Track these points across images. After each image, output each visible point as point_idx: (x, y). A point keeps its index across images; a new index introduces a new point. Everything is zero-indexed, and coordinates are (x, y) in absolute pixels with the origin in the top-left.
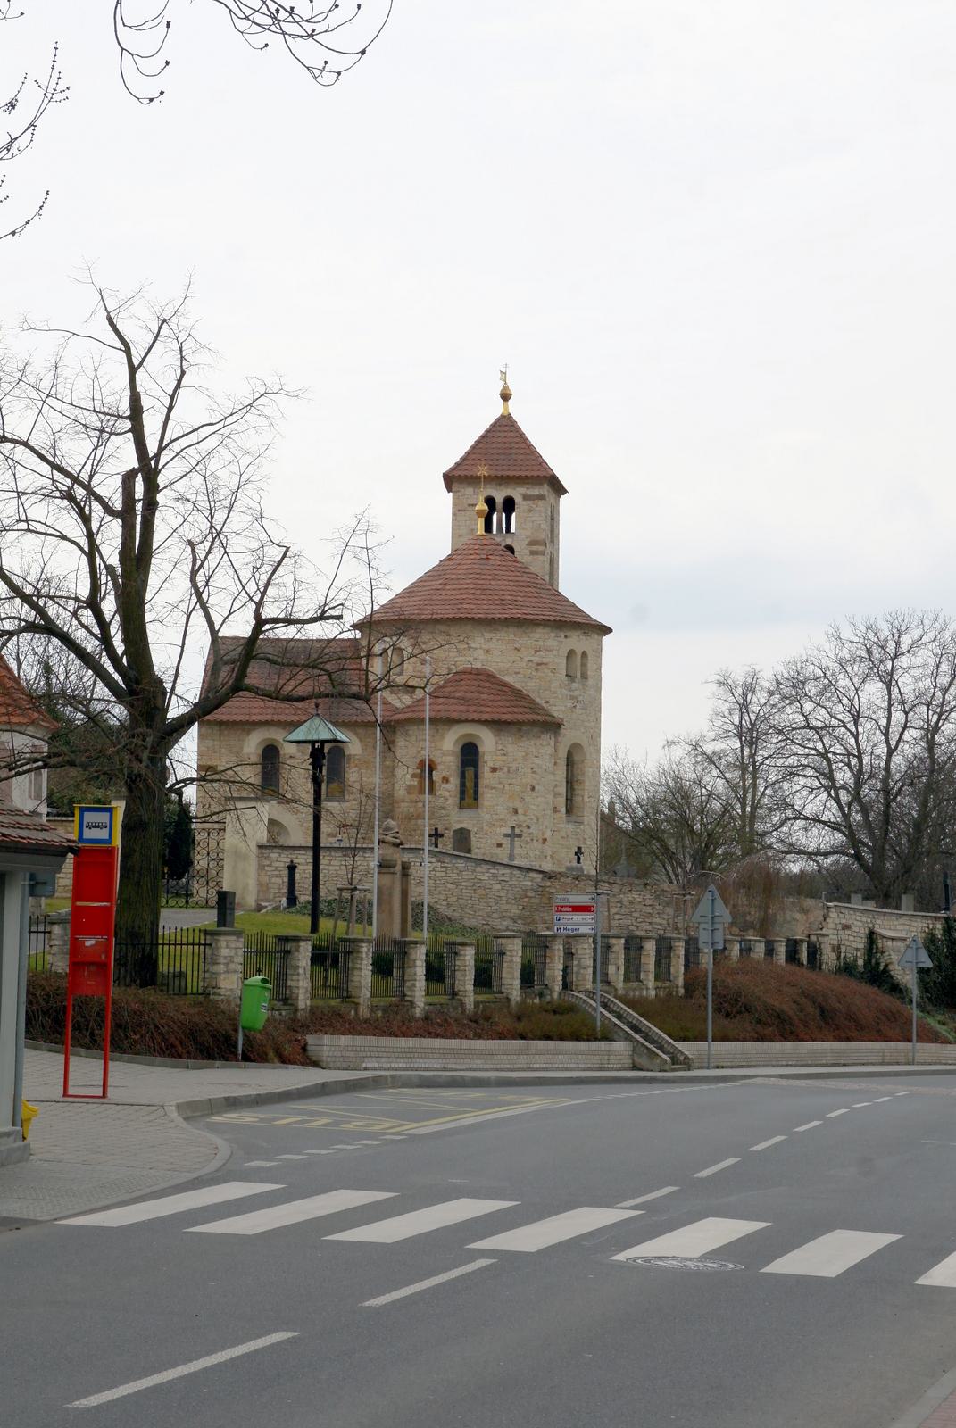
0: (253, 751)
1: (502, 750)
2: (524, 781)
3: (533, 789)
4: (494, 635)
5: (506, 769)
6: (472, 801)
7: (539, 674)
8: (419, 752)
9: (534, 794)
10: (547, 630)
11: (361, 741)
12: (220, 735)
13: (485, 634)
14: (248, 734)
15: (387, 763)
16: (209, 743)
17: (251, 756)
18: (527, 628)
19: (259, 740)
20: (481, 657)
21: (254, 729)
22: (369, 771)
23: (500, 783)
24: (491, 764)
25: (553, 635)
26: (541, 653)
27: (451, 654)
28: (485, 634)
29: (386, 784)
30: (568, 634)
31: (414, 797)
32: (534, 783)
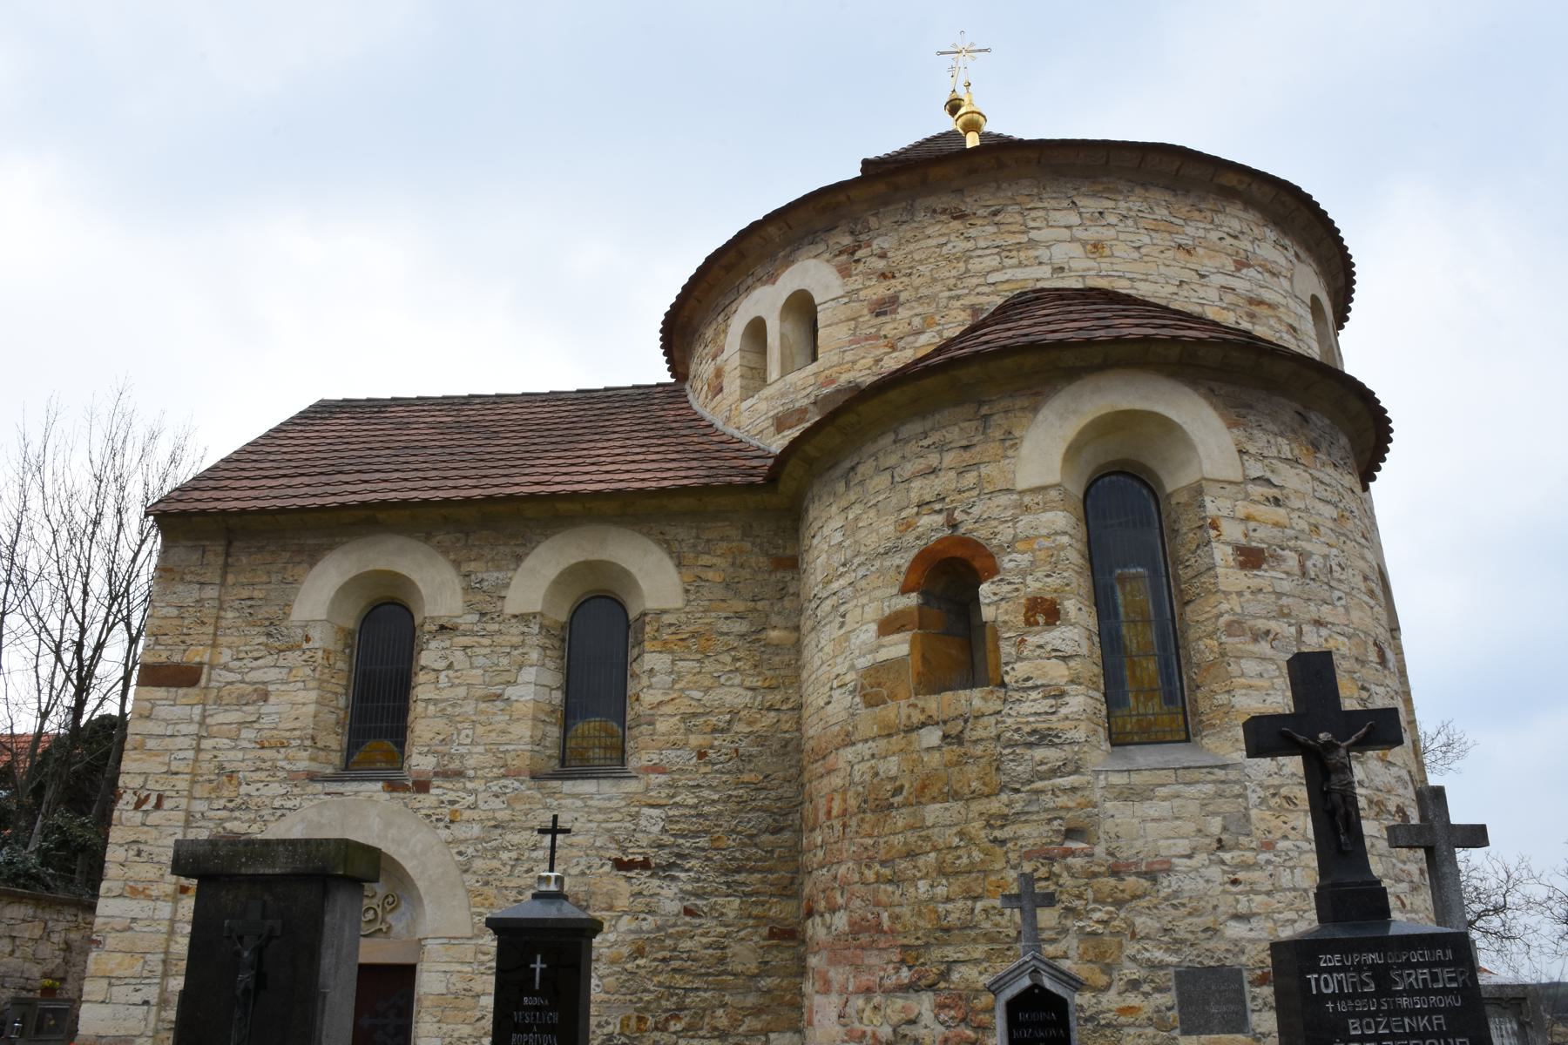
0: (321, 613)
2: (1356, 615)
4: (1111, 204)
6: (1154, 706)
8: (907, 525)
10: (1251, 216)
11: (679, 565)
12: (226, 566)
13: (1081, 201)
14: (312, 566)
15: (774, 634)
16: (187, 594)
17: (316, 634)
18: (1203, 199)
19: (347, 578)
20: (1075, 264)
21: (331, 548)
22: (709, 666)
23: (1283, 614)
24: (1233, 532)
26: (1251, 272)
27: (975, 265)
28: (1081, 201)
29: (770, 709)
30: (1303, 254)
31: (898, 710)
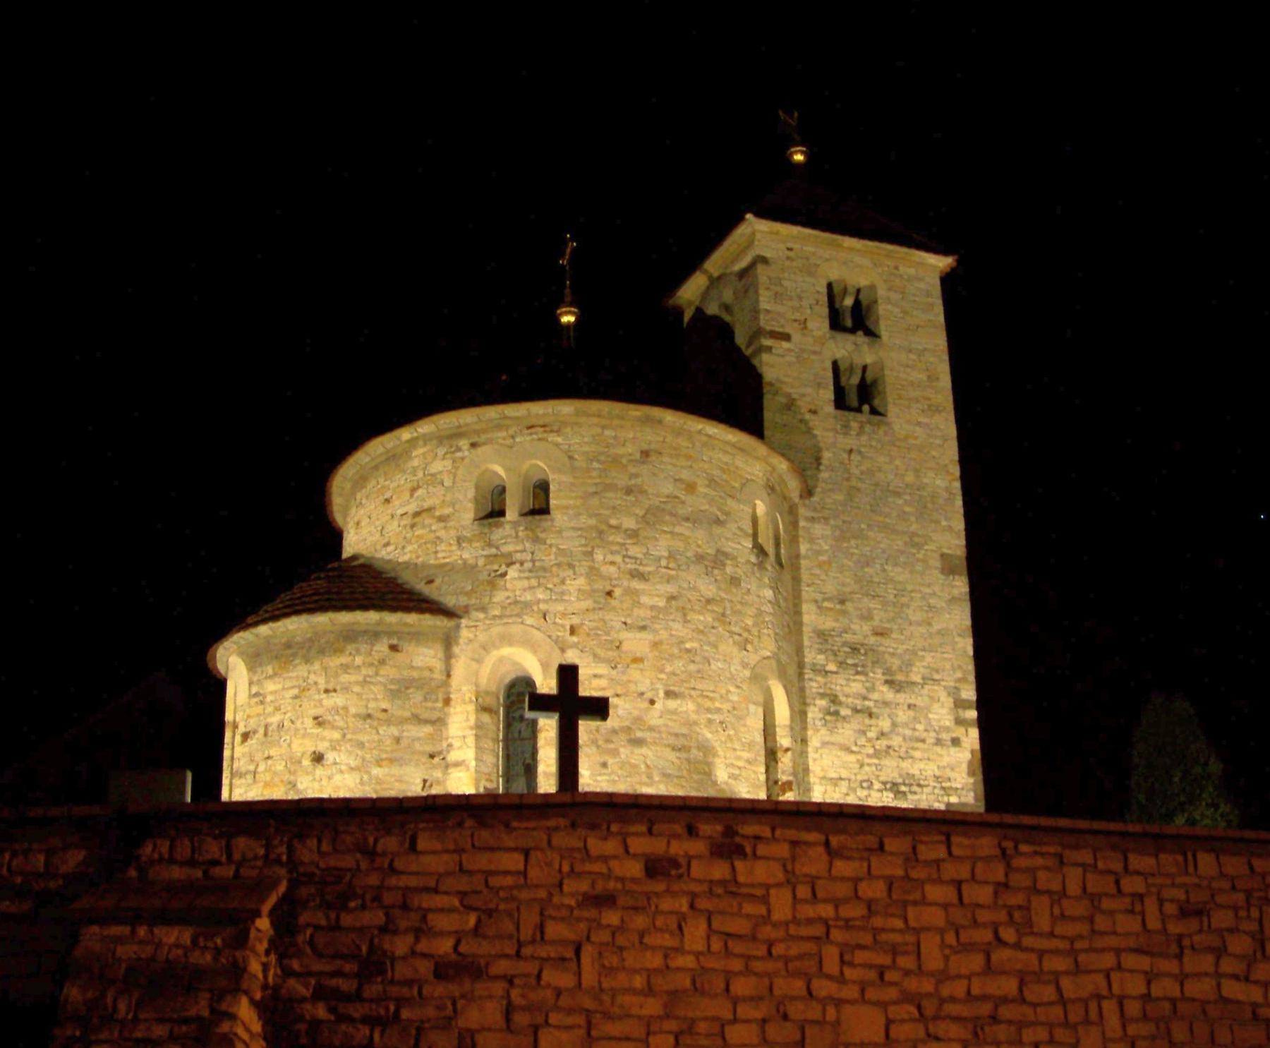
1: (256, 695)
3: (318, 758)
5: (262, 731)
7: (419, 532)
9: (320, 771)
25: (441, 451)
26: (420, 492)
32: (322, 747)
